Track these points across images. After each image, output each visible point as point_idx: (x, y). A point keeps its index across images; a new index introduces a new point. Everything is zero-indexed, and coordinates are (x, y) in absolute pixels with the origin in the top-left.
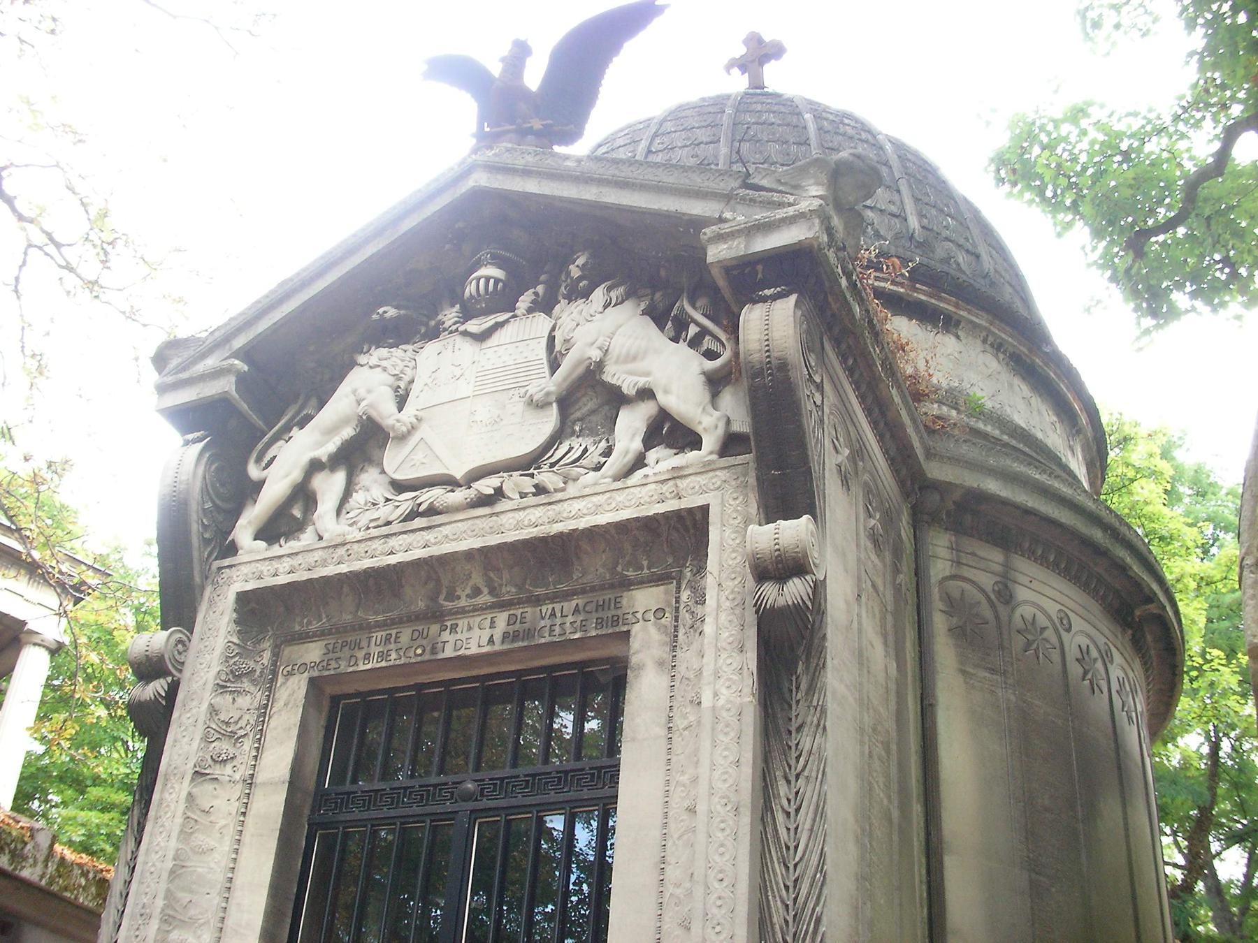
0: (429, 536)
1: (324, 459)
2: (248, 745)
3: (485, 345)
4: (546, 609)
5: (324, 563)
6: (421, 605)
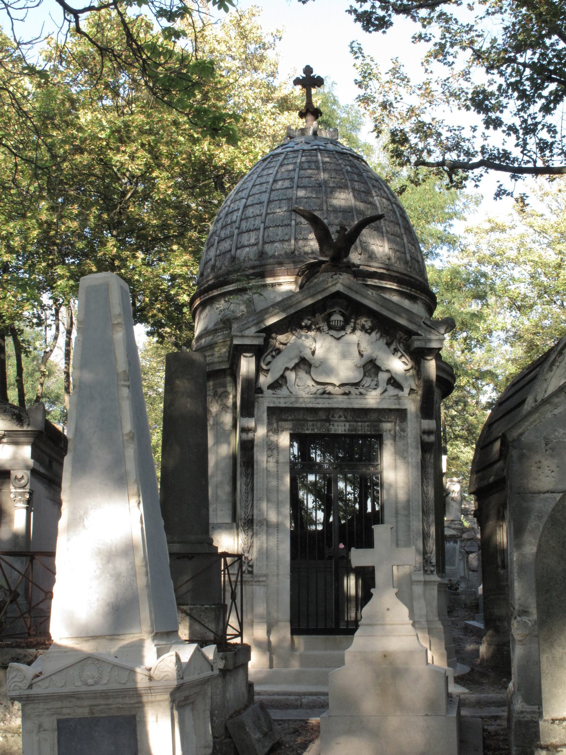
0: (330, 401)
3: (340, 341)
4: (360, 424)
6: (324, 418)
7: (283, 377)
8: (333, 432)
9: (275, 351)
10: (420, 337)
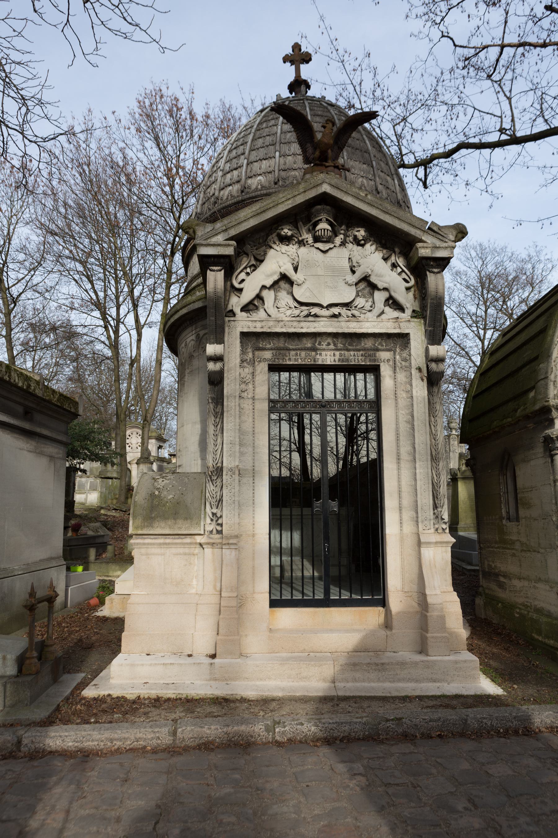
0: (316, 324)
1: (268, 286)
2: (250, 386)
5: (275, 327)
7: (259, 297)
8: (320, 362)
9: (250, 267)
10: (425, 245)
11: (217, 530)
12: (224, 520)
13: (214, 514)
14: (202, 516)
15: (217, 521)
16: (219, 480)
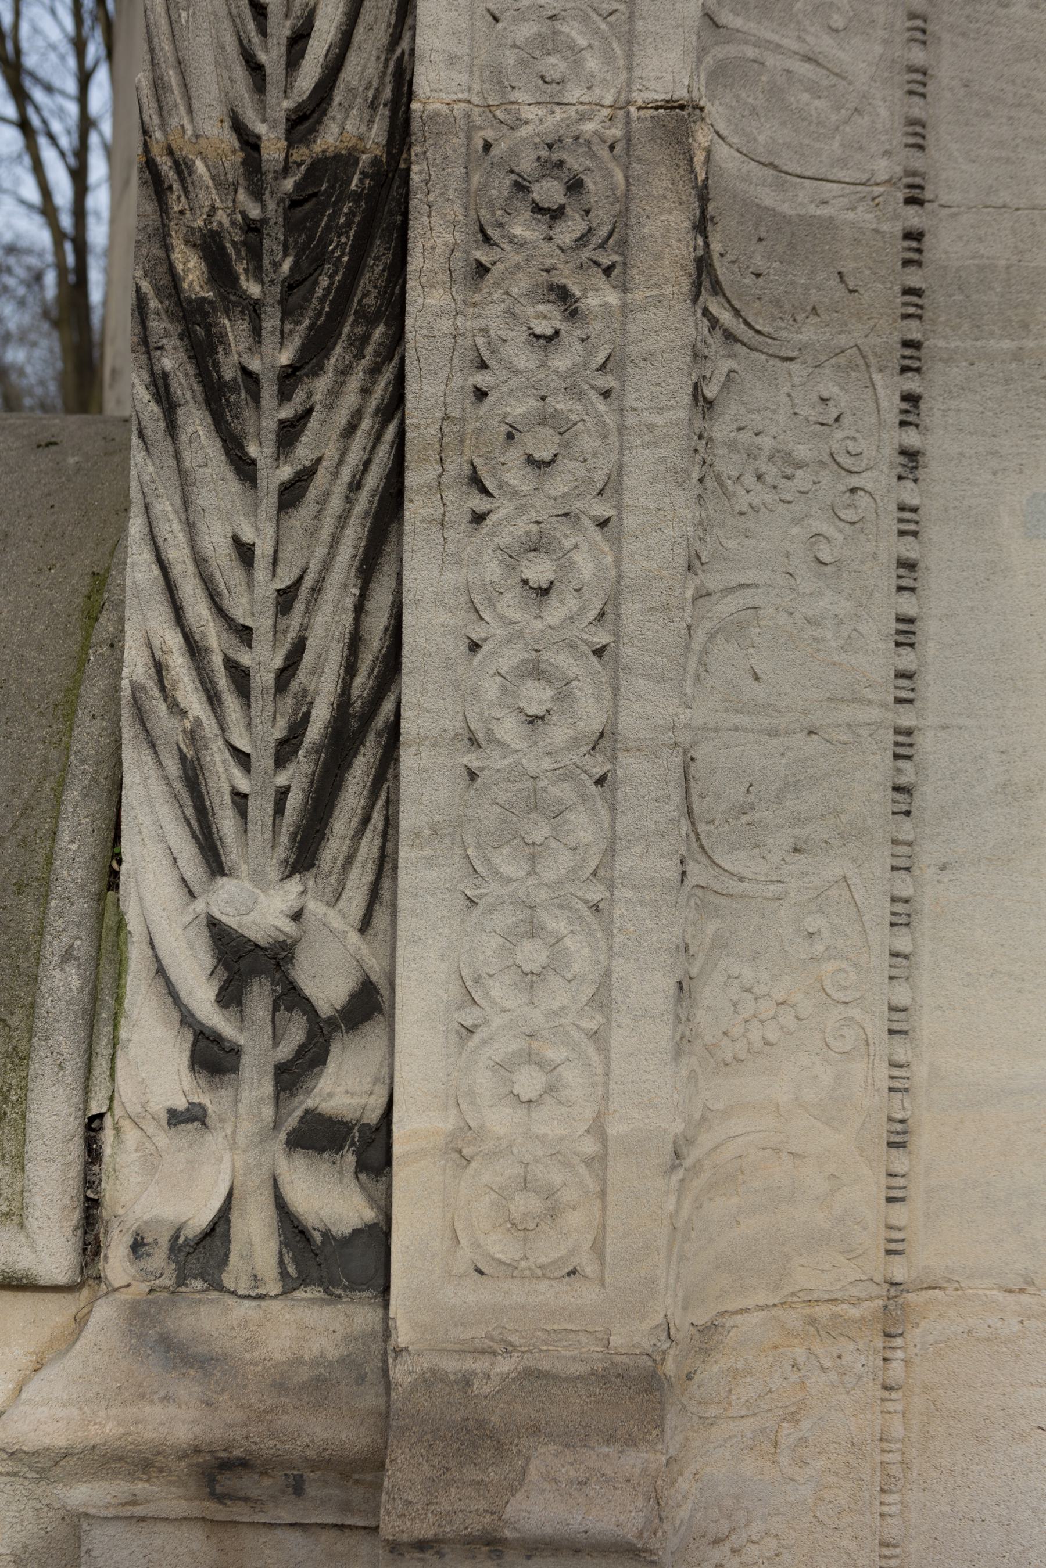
11: (292, 1229)
12: (420, 1074)
13: (245, 963)
14: (63, 982)
15: (290, 1077)
16: (339, 394)
